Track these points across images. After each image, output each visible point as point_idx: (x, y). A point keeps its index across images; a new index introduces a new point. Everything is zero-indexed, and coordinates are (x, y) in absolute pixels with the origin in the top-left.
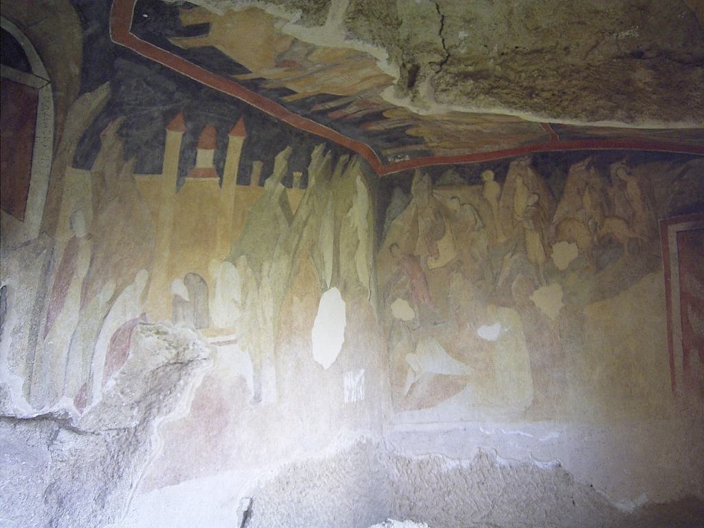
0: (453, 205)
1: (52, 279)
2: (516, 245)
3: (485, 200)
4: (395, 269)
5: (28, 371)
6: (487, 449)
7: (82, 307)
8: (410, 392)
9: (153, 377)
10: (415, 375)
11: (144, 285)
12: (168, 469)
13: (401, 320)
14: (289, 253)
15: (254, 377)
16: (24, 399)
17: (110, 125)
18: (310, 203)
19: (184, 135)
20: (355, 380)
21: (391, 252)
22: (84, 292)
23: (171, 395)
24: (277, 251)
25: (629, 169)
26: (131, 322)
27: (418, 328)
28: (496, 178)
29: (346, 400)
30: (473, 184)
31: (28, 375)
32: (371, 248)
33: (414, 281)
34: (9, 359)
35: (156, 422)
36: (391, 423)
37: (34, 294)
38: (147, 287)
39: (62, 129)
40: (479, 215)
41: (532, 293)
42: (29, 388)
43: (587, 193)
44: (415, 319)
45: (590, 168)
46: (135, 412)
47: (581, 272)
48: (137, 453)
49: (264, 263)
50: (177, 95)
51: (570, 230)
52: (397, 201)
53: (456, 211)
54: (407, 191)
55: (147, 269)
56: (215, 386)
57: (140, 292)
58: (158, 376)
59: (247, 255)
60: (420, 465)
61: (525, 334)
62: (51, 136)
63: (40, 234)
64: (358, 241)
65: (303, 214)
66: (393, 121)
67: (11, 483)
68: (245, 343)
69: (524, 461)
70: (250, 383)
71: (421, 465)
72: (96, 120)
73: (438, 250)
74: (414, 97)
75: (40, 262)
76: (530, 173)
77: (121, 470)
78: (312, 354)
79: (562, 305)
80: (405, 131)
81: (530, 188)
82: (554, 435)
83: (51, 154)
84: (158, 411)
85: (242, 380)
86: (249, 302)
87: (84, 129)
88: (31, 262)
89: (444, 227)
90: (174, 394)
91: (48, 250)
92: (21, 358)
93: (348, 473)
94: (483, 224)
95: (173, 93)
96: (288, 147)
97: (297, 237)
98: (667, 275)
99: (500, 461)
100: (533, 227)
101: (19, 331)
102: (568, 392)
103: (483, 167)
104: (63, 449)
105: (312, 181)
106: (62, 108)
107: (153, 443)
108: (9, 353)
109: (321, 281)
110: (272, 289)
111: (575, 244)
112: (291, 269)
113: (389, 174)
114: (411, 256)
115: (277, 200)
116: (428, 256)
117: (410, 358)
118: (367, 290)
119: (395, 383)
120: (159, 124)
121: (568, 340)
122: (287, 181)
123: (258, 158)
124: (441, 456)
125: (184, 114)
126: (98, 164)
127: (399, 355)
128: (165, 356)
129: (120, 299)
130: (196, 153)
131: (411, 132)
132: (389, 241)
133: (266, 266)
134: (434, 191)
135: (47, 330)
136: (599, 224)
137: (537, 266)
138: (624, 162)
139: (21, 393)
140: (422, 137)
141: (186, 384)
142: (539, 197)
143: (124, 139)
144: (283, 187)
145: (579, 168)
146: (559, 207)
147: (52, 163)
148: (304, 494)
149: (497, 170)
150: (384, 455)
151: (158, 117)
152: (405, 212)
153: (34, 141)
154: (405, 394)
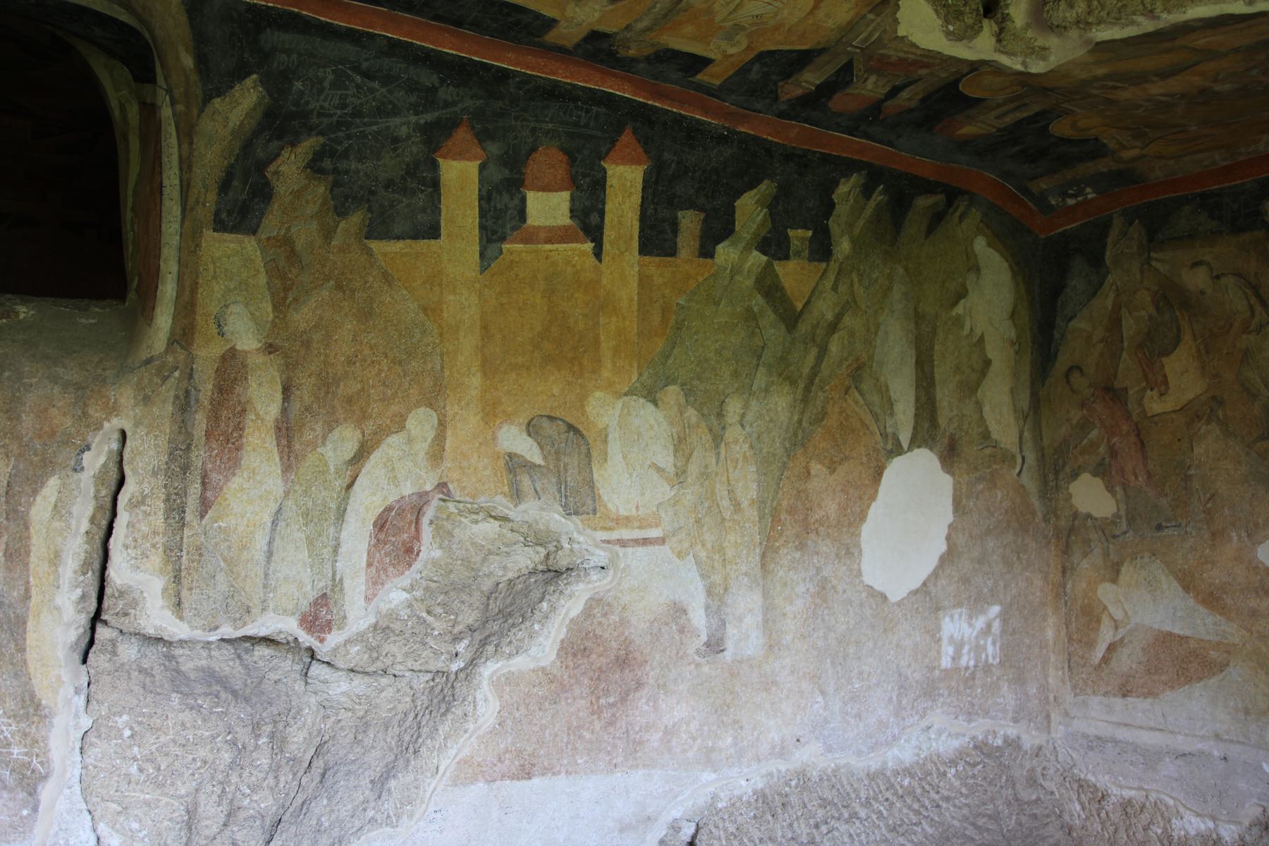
0: (1197, 280)
1: (200, 422)
4: (1076, 415)
5: (170, 568)
7: (287, 469)
8: (1106, 660)
9: (508, 590)
10: (1116, 628)
11: (431, 435)
12: (506, 751)
13: (1089, 516)
14: (793, 382)
15: (707, 607)
16: (168, 614)
17: (285, 154)
18: (843, 288)
19: (482, 168)
20: (971, 625)
21: (1068, 382)
22: (284, 442)
23: (523, 626)
24: (761, 379)
26: (415, 497)
27: (1125, 533)
29: (946, 662)
31: (172, 574)
32: (1025, 377)
34: (126, 547)
35: (489, 669)
36: (1067, 714)
37: (163, 442)
38: (440, 438)
39: (190, 167)
40: (1258, 296)
42: (178, 594)
44: (1117, 515)
46: (461, 647)
48: (450, 716)
49: (727, 400)
50: (445, 93)
52: (1076, 283)
53: (1202, 293)
54: (1096, 261)
55: (431, 406)
56: (614, 618)
57: (422, 447)
58: (514, 590)
59: (682, 385)
62: (177, 182)
63: (168, 344)
64: (987, 363)
65: (825, 308)
66: (999, 106)
67: (173, 741)
68: (686, 545)
70: (698, 618)
71: (1129, 810)
72: (247, 147)
73: (1165, 376)
74: (1002, 30)
75: (169, 391)
77: (420, 740)
78: (860, 570)
80: (1046, 127)
83: (179, 213)
84: (496, 651)
85: (679, 610)
86: (694, 469)
87: (226, 162)
88: (153, 391)
89: (1179, 330)
90: (528, 624)
91: (182, 371)
92: (154, 546)
93: (947, 799)
95: (433, 90)
96: (766, 182)
97: (814, 352)
101: (143, 502)
104: (330, 693)
105: (843, 246)
106: (187, 133)
107: (480, 703)
108: (126, 537)
109: (885, 436)
110: (752, 447)
112: (803, 413)
113: (1060, 230)
115: (750, 282)
116: (1144, 390)
117: (1106, 592)
118: (1013, 457)
119: (1075, 637)
120: (415, 149)
122: (774, 245)
123: (691, 205)
125: (473, 128)
126: (272, 223)
127: (1084, 585)
128: (525, 559)
129: (376, 457)
130: (523, 200)
131: (1060, 128)
132: (1063, 362)
133: (734, 407)
135: (205, 506)
139: (160, 602)
140: (1097, 139)
141: (553, 608)
143: (331, 178)
144: (765, 258)
147: (182, 226)
148: (824, 829)
150: (1051, 771)
151: (409, 137)
153: (161, 195)
154: (1097, 661)
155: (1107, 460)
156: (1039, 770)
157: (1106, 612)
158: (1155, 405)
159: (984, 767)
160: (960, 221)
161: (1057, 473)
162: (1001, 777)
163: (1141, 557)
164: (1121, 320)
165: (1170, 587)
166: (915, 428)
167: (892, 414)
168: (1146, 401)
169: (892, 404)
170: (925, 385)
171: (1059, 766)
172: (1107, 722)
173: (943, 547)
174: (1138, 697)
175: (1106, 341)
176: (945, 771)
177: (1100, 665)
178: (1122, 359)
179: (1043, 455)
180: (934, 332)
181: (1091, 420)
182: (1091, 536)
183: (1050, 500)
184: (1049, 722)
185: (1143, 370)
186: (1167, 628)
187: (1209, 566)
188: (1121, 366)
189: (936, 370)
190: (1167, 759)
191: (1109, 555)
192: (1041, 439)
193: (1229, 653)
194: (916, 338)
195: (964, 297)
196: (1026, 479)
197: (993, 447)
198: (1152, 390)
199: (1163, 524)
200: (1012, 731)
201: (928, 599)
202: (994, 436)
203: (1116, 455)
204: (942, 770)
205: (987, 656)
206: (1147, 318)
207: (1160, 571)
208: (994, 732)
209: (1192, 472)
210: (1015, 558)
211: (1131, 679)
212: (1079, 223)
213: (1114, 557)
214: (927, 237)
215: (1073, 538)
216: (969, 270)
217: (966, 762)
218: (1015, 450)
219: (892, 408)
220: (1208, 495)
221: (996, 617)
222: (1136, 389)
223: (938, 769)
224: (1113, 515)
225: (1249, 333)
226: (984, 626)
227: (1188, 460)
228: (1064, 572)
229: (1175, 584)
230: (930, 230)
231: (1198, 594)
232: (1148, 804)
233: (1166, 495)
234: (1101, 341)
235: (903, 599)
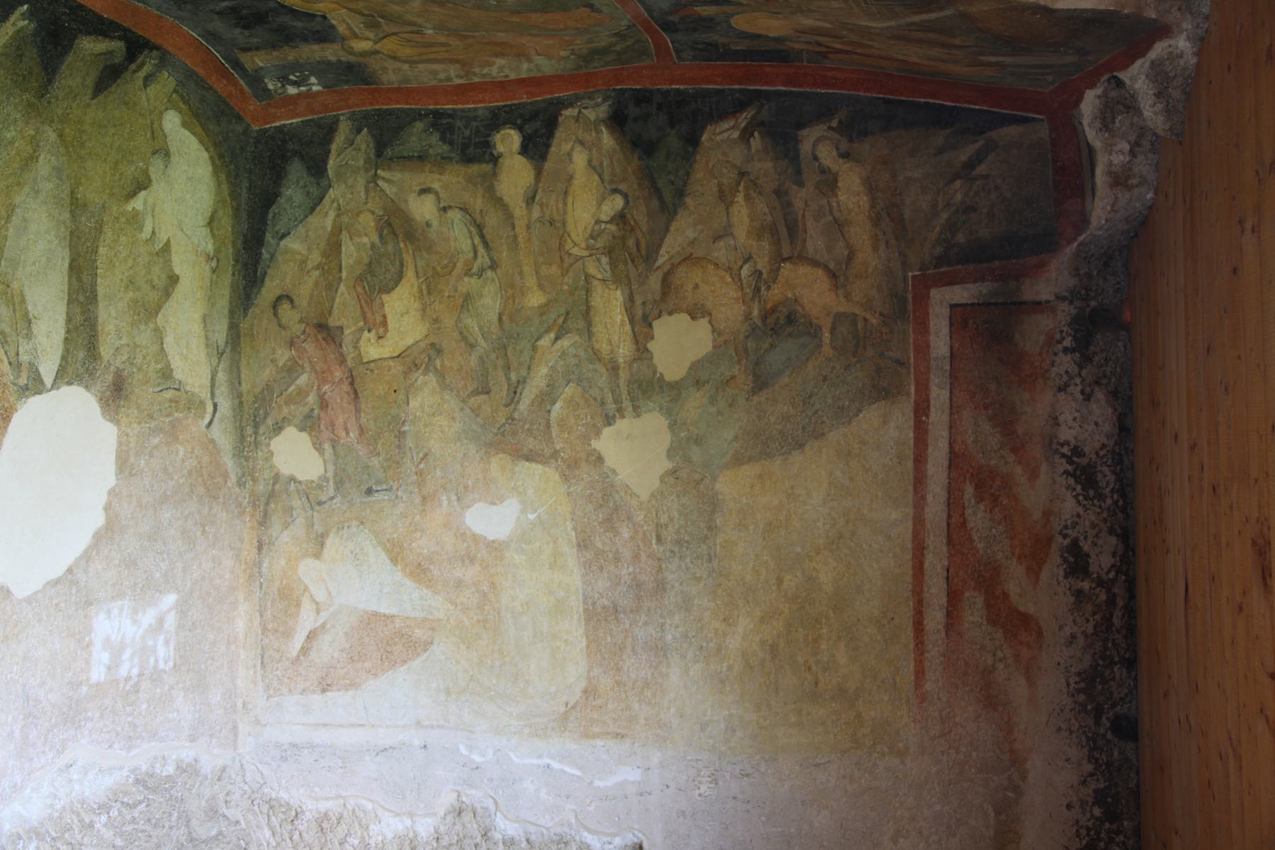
0: (423, 209)
2: (568, 313)
3: (499, 202)
4: (283, 355)
6: (474, 796)
8: (305, 651)
10: (318, 612)
13: (292, 479)
20: (135, 622)
21: (275, 314)
25: (844, 145)
27: (332, 498)
28: (524, 150)
30: (468, 160)
32: (223, 303)
33: (326, 388)
36: (257, 722)
40: (482, 236)
41: (598, 433)
43: (740, 198)
45: (752, 135)
47: (717, 390)
51: (696, 286)
52: (293, 192)
53: (428, 224)
54: (317, 169)
60: (323, 822)
61: (575, 529)
64: (174, 280)
69: (558, 830)
71: (325, 825)
73: (384, 317)
76: (607, 139)
79: (668, 465)
81: (606, 177)
82: (630, 774)
89: (402, 265)
94: (491, 259)
98: (921, 409)
99: (505, 826)
100: (608, 275)
102: (667, 675)
103: (497, 121)
109: (16, 366)
111: (707, 319)
113: (278, 124)
114: (322, 327)
116: (361, 330)
117: (308, 570)
118: (202, 403)
121: (676, 549)
124: (369, 806)
127: (283, 562)
132: (270, 289)
134: (379, 172)
136: (765, 276)
137: (614, 369)
138: (834, 124)
140: (324, 17)
142: (627, 202)
145: (726, 135)
146: (672, 228)
149: (529, 129)
152: (313, 220)
154: (294, 653)
155: (316, 412)
156: (221, 796)
157: (307, 594)
158: (373, 350)
159: (148, 805)
160: (145, 86)
161: (256, 426)
162: (170, 815)
163: (348, 527)
164: (340, 245)
165: (377, 559)
166: (64, 358)
167: (29, 336)
168: (361, 343)
169: (30, 322)
170: (81, 298)
171: (246, 788)
172: (303, 724)
173: (100, 520)
174: (339, 690)
175: (323, 268)
176: (92, 821)
177: (298, 657)
178: (339, 291)
179: (241, 403)
180: (99, 229)
181: (300, 362)
182: (293, 503)
183: (247, 459)
184: (236, 735)
185: (362, 307)
186: (373, 607)
187: (418, 534)
188: (338, 300)
189: (99, 280)
190: (367, 758)
191: (313, 525)
192: (240, 383)
193: (433, 629)
194: (72, 233)
195: (145, 189)
196: (216, 432)
197: (176, 389)
198: (369, 331)
199: (374, 488)
200: (187, 754)
201: (74, 590)
202: (178, 375)
203: (327, 406)
204: (87, 820)
205: (156, 661)
206: (369, 246)
207: (368, 542)
208: (164, 758)
209: (406, 428)
210: (199, 533)
211: (332, 670)
212: (300, 120)
213: (318, 528)
214: (95, 96)
215: (272, 506)
216: (154, 154)
217: (122, 803)
218: (205, 395)
219: (29, 328)
220: (421, 455)
221: (171, 609)
222: (353, 329)
223: (81, 821)
224: (320, 478)
225: (471, 276)
226: (153, 621)
227: (403, 415)
228: (260, 548)
229: (383, 556)
230: (100, 87)
231: (406, 566)
232: (345, 814)
233: (378, 454)
234: (317, 268)
235: (36, 593)
